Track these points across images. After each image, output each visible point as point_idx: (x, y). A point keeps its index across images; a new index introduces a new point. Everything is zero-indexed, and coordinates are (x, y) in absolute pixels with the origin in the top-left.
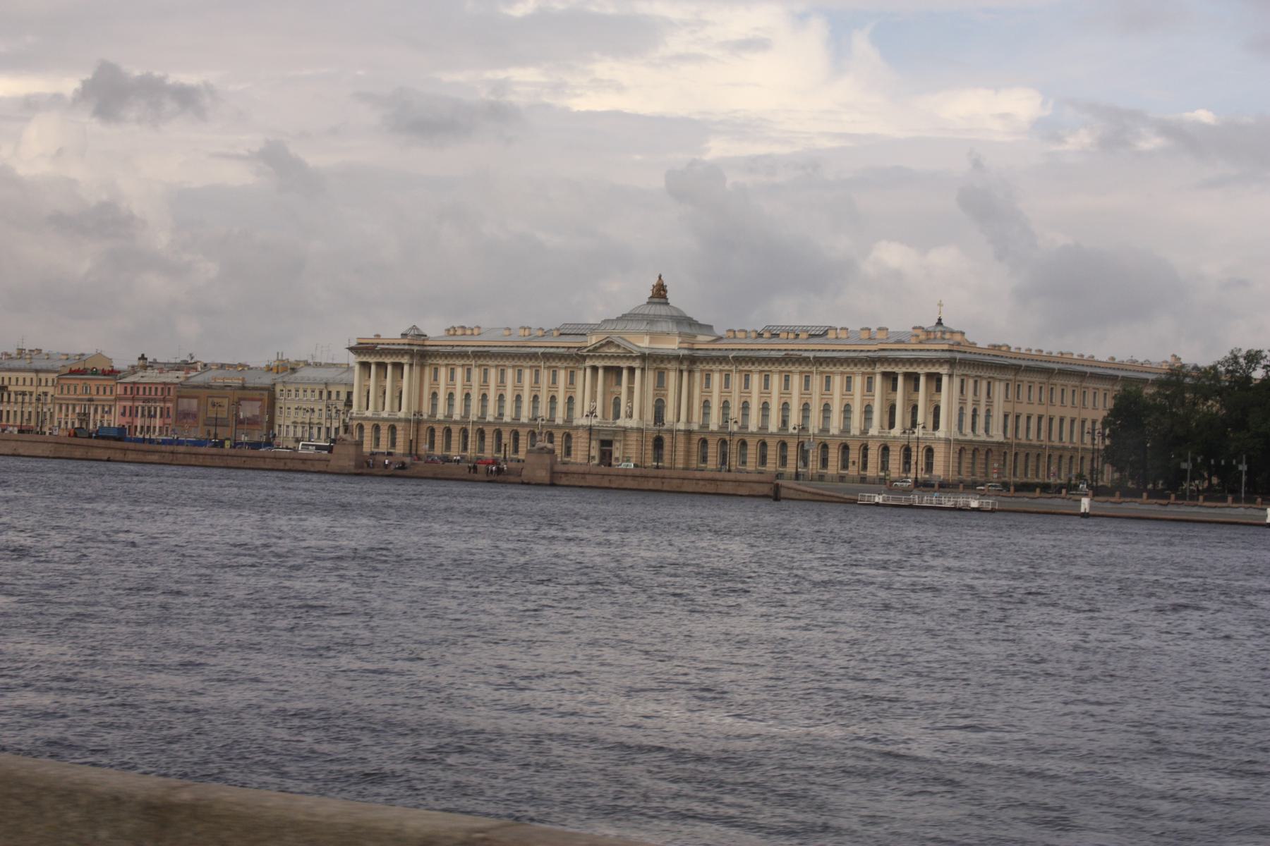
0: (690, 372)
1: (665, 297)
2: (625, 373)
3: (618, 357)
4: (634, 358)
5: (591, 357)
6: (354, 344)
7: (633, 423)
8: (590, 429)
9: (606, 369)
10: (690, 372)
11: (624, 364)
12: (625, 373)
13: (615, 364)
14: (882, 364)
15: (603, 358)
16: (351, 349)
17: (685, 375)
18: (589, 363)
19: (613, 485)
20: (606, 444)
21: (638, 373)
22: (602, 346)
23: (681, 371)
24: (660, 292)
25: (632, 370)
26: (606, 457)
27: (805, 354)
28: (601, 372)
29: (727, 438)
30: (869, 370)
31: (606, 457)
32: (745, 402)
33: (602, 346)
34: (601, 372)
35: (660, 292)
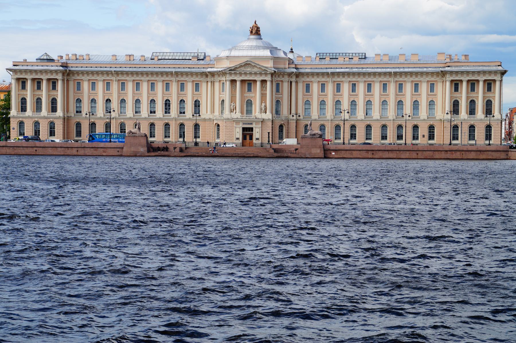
0: (297, 82)
2: (258, 84)
3: (256, 73)
4: (266, 74)
5: (230, 74)
9: (242, 81)
10: (297, 82)
11: (259, 78)
13: (251, 78)
14: (451, 75)
15: (241, 74)
16: (11, 70)
17: (294, 84)
18: (229, 78)
19: (376, 156)
21: (269, 84)
22: (241, 66)
23: (291, 82)
25: (264, 82)
28: (238, 84)
33: (241, 66)
34: (238, 84)
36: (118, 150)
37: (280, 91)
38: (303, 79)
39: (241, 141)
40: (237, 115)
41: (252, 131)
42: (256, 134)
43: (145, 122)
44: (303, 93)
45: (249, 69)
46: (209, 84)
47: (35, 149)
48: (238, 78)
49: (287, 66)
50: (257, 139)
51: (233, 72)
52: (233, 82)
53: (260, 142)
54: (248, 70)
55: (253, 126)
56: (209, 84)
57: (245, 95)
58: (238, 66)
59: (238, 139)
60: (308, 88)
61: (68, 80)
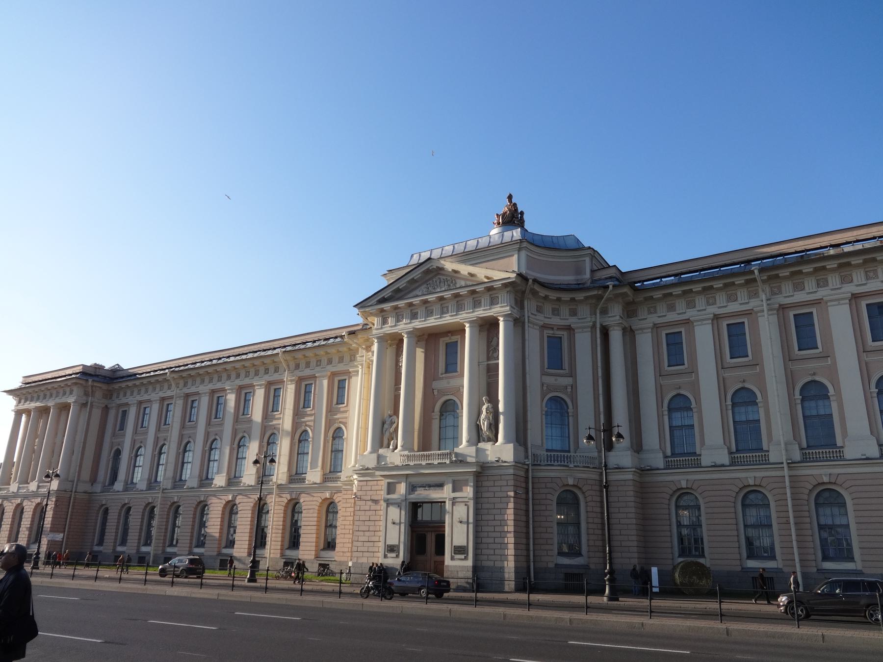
0: (629, 334)
6: (17, 384)
10: (629, 334)
16: (10, 392)
17: (616, 337)
23: (605, 333)
25: (489, 327)
35: (513, 218)
37: (566, 365)
38: (654, 319)
44: (658, 366)
49: (588, 275)
50: (460, 550)
51: (387, 306)
53: (469, 563)
55: (446, 493)
57: (436, 385)
58: (401, 284)
59: (392, 549)
60: (675, 347)
61: (106, 409)
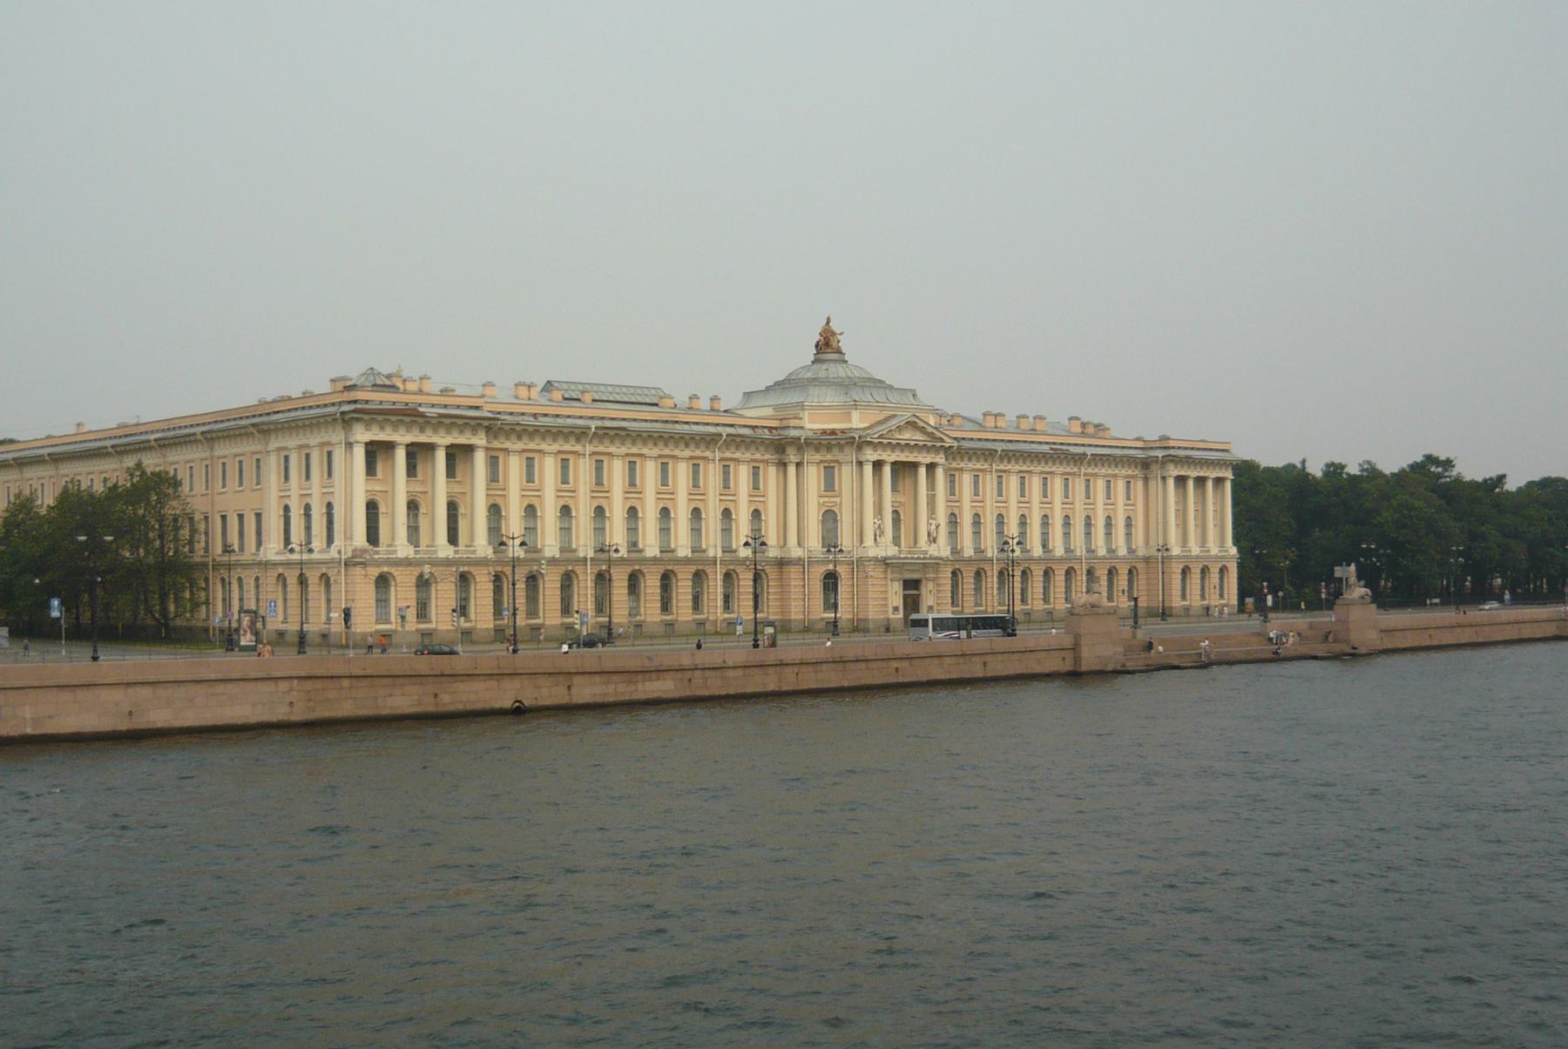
1: (839, 351)
2: (922, 471)
7: (942, 549)
8: (885, 562)
11: (924, 458)
12: (922, 471)
13: (911, 458)
15: (893, 447)
18: (871, 455)
20: (912, 585)
21: (940, 472)
24: (827, 345)
25: (931, 467)
26: (912, 603)
27: (1073, 450)
28: (887, 470)
29: (508, 570)
30: (258, 447)
31: (912, 603)
32: (1000, 515)
34: (887, 470)
36: (1063, 653)
39: (901, 615)
40: (887, 549)
41: (917, 588)
42: (928, 597)
43: (654, 569)
45: (907, 435)
46: (792, 470)
47: (894, 664)
48: (890, 457)
50: (930, 608)
52: (878, 465)
54: (907, 436)
56: (792, 470)
59: (896, 609)
